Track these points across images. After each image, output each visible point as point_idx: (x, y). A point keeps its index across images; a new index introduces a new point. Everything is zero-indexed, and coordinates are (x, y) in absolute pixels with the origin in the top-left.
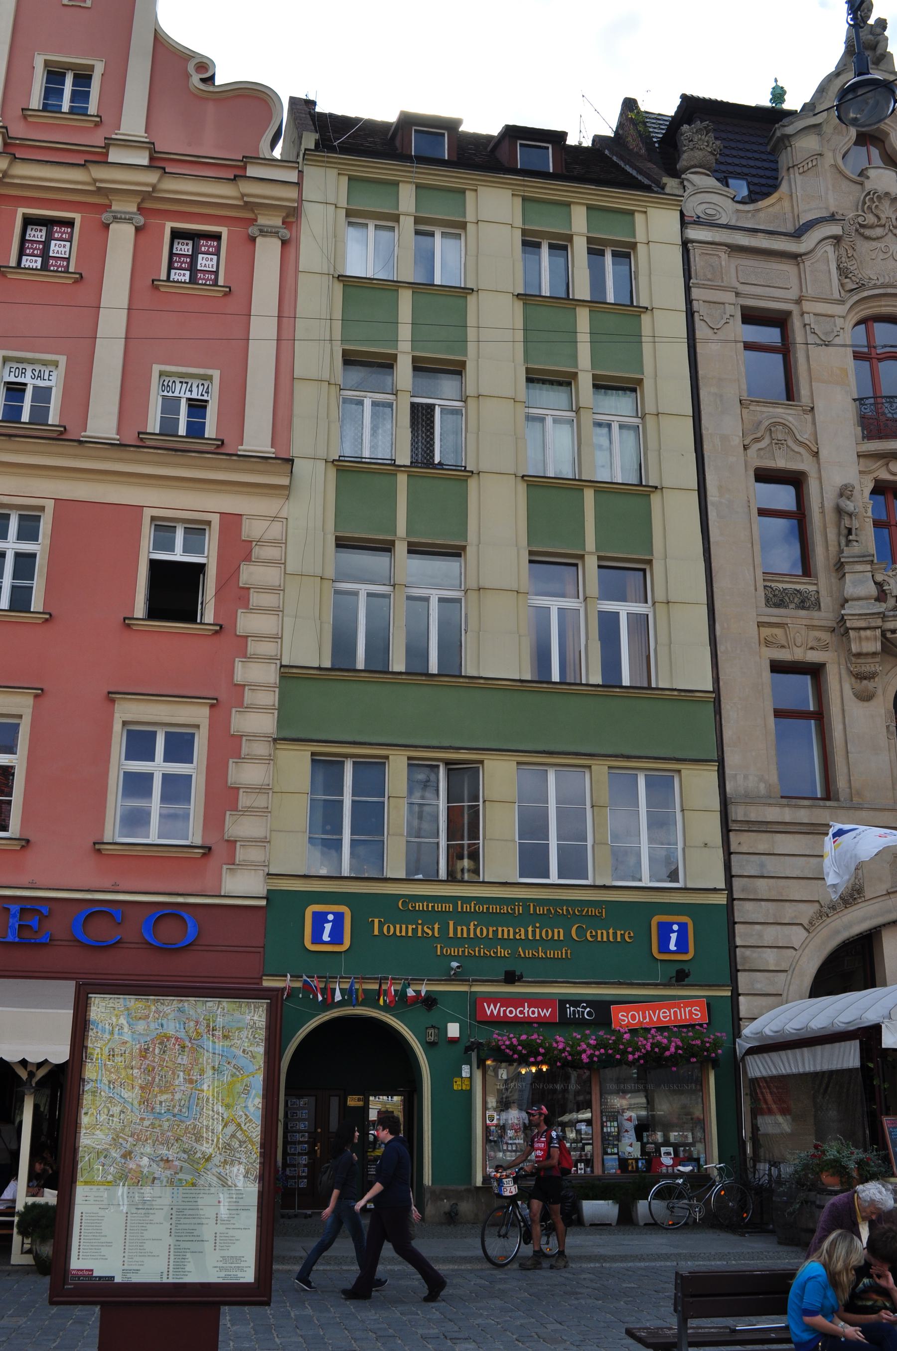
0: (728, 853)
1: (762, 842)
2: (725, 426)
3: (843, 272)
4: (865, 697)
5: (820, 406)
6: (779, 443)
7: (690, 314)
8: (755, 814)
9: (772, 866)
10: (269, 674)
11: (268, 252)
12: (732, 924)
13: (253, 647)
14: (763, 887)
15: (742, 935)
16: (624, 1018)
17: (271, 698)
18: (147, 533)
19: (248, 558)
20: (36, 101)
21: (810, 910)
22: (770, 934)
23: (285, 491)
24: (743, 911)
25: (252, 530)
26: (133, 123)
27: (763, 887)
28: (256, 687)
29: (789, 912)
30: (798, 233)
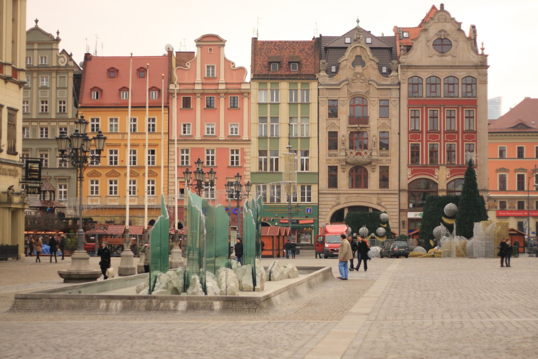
0: (319, 197)
1: (324, 196)
2: (323, 125)
3: (348, 90)
4: (343, 172)
5: (341, 119)
6: (333, 127)
7: (318, 103)
8: (322, 192)
9: (325, 199)
10: (249, 173)
11: (246, 100)
12: (318, 208)
13: (247, 169)
14: (324, 203)
15: (320, 210)
16: (301, 222)
17: (249, 177)
18: (230, 152)
19: (245, 155)
20: (206, 76)
21: (331, 206)
22: (324, 210)
23: (250, 144)
24: (320, 206)
25: (246, 150)
26: (222, 79)
27: (324, 203)
28: (247, 175)
29: (327, 206)
30: (339, 85)
